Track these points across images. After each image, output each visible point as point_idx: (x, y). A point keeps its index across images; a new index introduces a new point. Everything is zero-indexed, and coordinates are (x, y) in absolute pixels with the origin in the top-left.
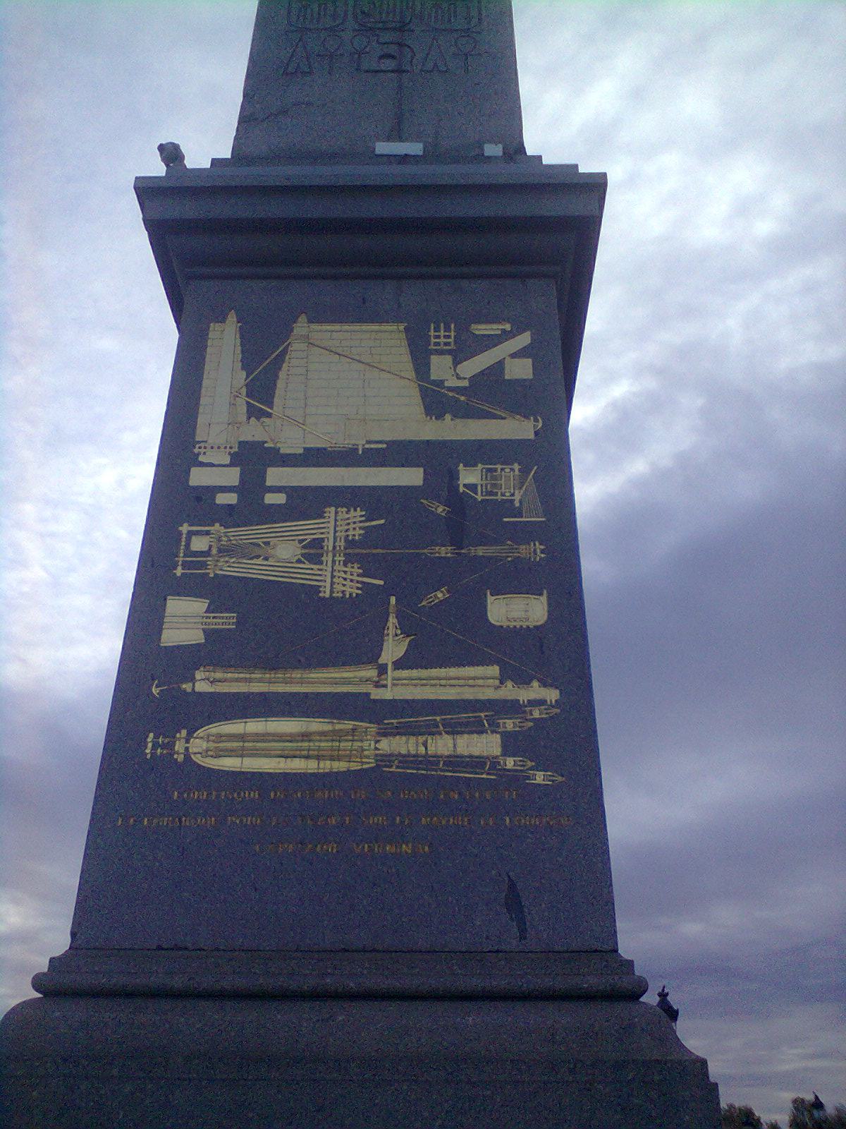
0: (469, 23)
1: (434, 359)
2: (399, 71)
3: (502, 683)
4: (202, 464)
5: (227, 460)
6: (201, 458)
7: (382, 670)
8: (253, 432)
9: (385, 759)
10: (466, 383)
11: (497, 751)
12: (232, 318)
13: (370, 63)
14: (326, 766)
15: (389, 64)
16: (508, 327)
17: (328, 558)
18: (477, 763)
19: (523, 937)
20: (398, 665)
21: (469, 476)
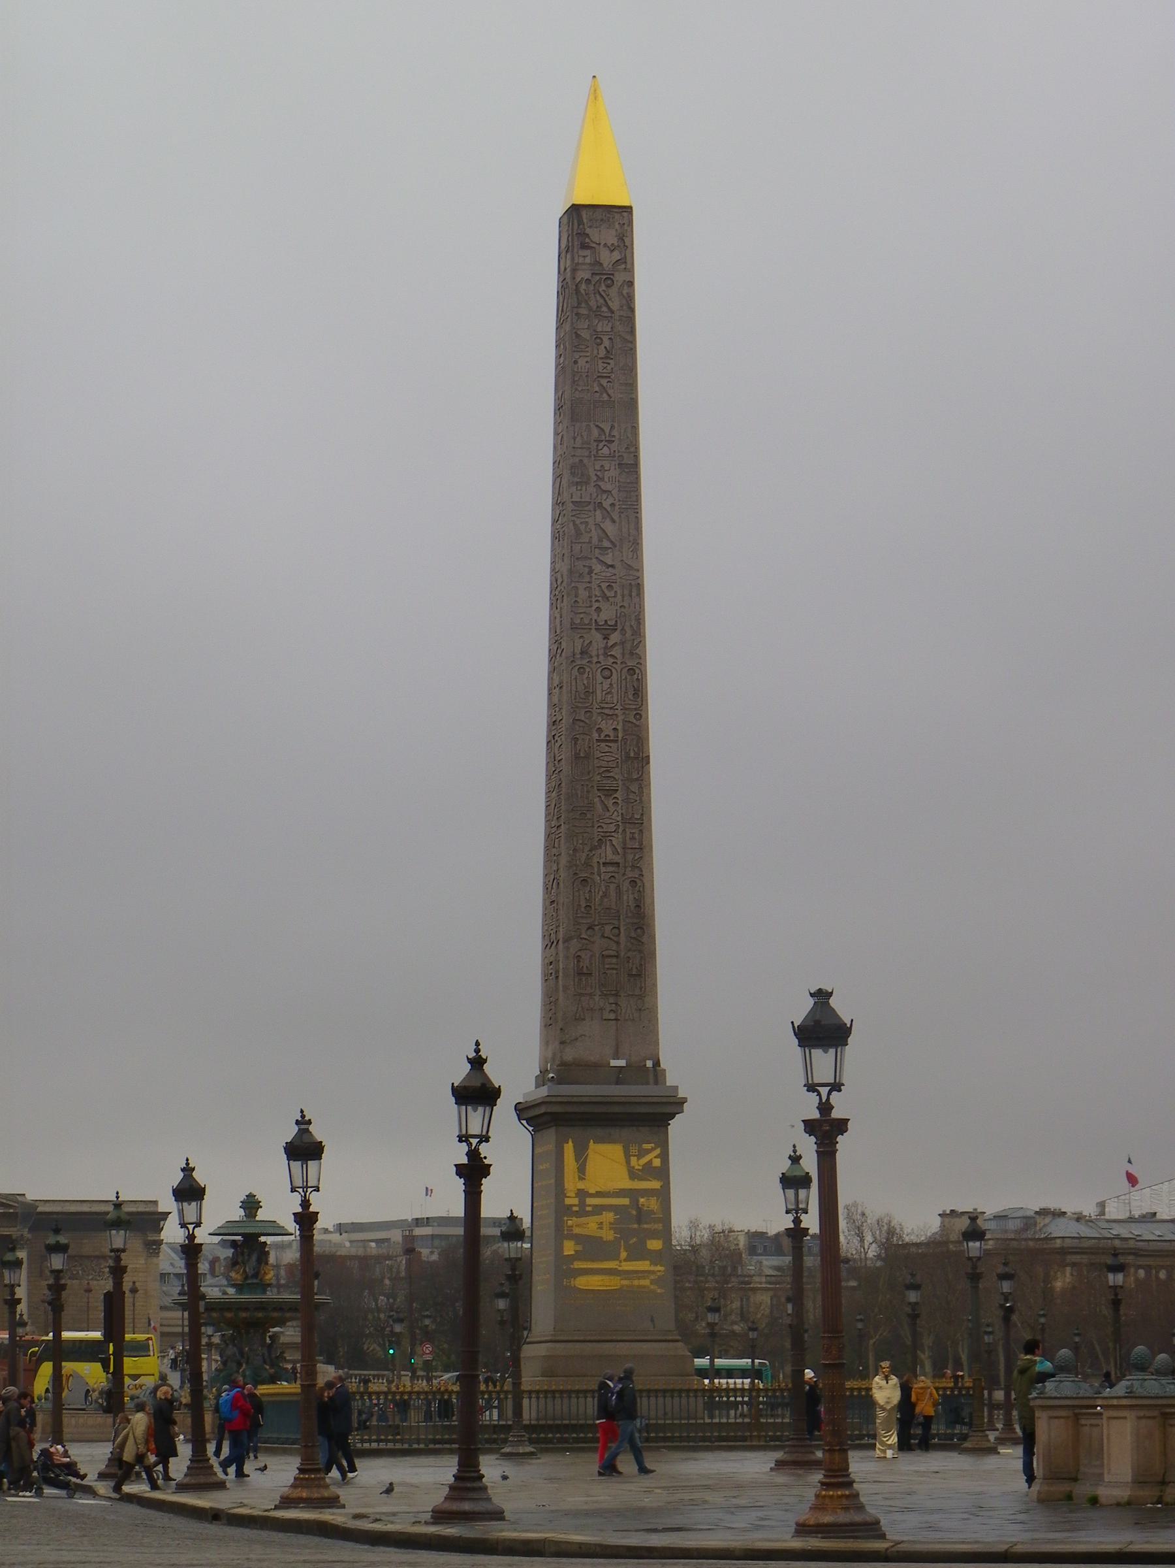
0: (641, 991)
1: (632, 1158)
2: (616, 1020)
3: (650, 1265)
4: (568, 1197)
5: (574, 1195)
6: (567, 1195)
7: (620, 1262)
8: (581, 1185)
9: (622, 1286)
10: (640, 1168)
11: (649, 1284)
12: (570, 1141)
13: (607, 1015)
14: (608, 1288)
15: (612, 1016)
16: (653, 1145)
17: (604, 1228)
18: (644, 1287)
19: (654, 1328)
20: (625, 1260)
21: (642, 1200)
